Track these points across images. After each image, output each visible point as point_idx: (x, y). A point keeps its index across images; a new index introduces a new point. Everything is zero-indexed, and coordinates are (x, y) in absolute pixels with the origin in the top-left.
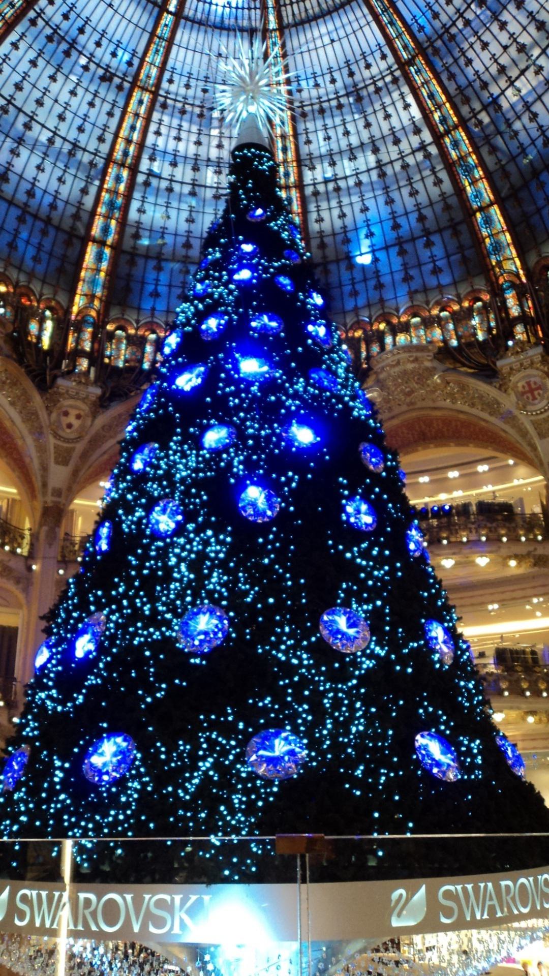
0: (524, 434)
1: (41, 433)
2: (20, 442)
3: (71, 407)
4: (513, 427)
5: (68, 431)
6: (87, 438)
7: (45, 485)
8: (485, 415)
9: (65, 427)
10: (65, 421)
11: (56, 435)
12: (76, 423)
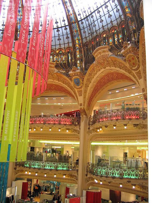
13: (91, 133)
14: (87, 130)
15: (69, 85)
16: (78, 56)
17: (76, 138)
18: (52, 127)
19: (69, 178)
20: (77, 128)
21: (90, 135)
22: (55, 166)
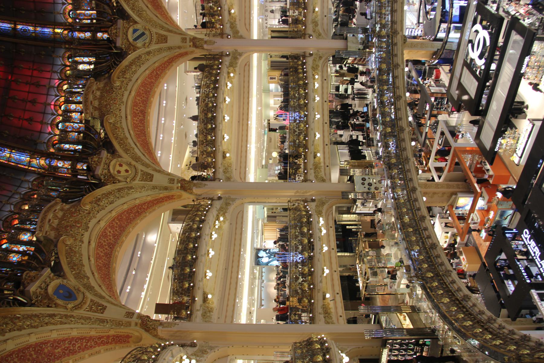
1: (131, 188)
2: (138, 202)
3: (114, 169)
5: (130, 172)
6: (134, 163)
7: (166, 188)
9: (127, 174)
11: (133, 179)
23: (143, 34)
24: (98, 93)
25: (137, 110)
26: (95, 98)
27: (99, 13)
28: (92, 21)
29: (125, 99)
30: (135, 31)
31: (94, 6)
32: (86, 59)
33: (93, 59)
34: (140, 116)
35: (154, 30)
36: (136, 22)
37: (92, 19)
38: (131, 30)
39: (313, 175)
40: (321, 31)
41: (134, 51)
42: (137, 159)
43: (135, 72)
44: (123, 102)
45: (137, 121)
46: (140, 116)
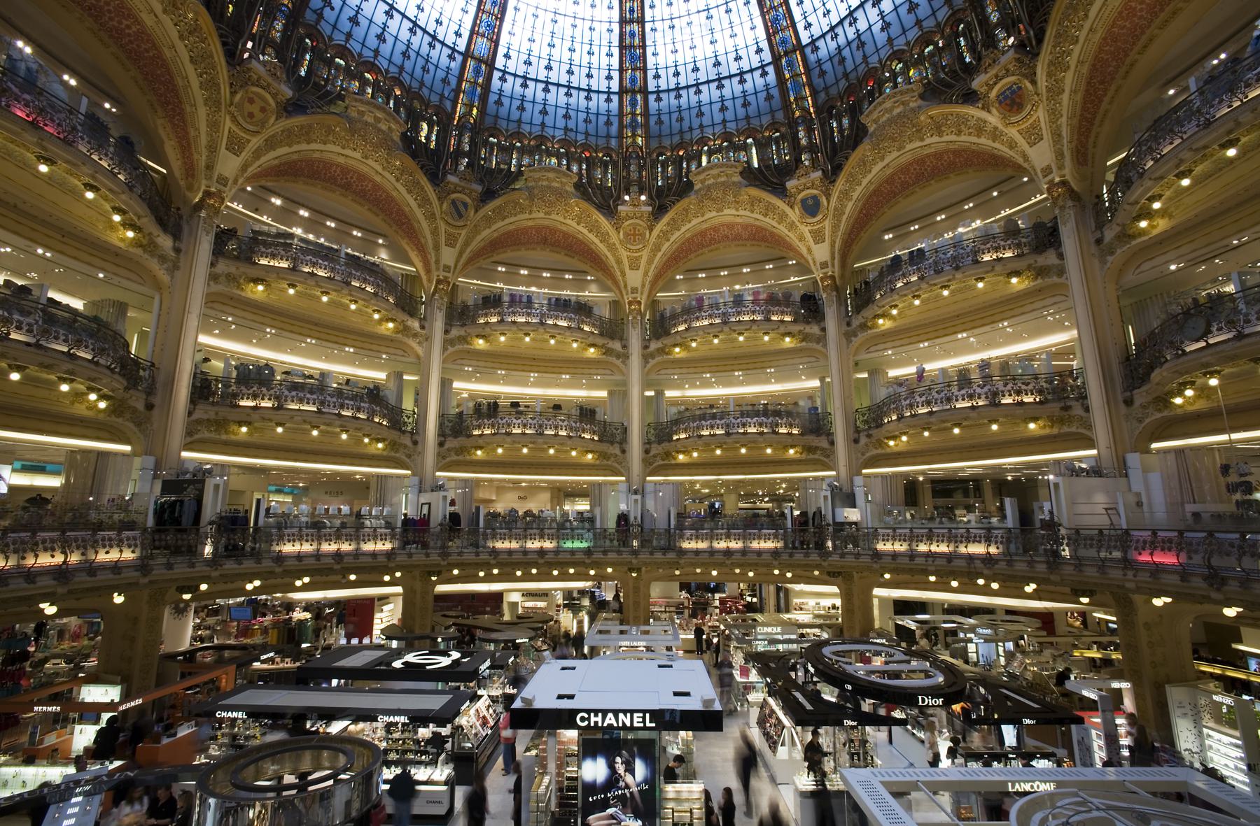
0: (619, 262)
4: (614, 255)
8: (596, 241)
10: (249, 108)
12: (259, 115)
13: (1112, 253)
14: (1094, 249)
15: (980, 129)
16: (994, 18)
17: (1054, 296)
18: (949, 281)
19: (1055, 431)
20: (1050, 258)
21: (1109, 264)
22: (986, 393)
23: (460, 216)
24: (384, 127)
25: (352, 178)
26: (378, 120)
27: (490, 171)
28: (482, 159)
29: (370, 162)
30: (466, 205)
31: (502, 166)
32: (434, 138)
33: (433, 145)
34: (342, 179)
35: (464, 232)
36: (476, 211)
37: (485, 159)
38: (468, 200)
39: (205, 417)
40: (448, 459)
41: (439, 199)
42: (271, 144)
43: (409, 192)
44: (366, 158)
45: (335, 171)
46: (342, 179)
